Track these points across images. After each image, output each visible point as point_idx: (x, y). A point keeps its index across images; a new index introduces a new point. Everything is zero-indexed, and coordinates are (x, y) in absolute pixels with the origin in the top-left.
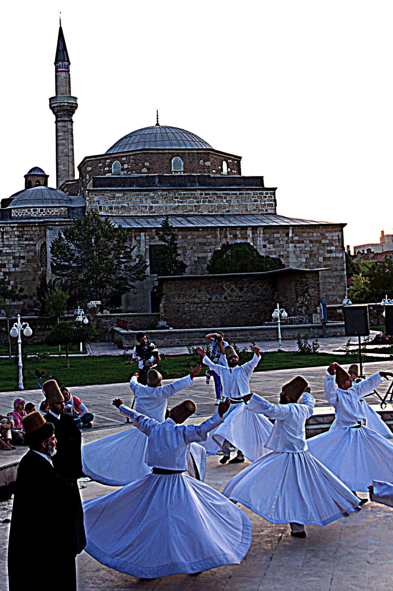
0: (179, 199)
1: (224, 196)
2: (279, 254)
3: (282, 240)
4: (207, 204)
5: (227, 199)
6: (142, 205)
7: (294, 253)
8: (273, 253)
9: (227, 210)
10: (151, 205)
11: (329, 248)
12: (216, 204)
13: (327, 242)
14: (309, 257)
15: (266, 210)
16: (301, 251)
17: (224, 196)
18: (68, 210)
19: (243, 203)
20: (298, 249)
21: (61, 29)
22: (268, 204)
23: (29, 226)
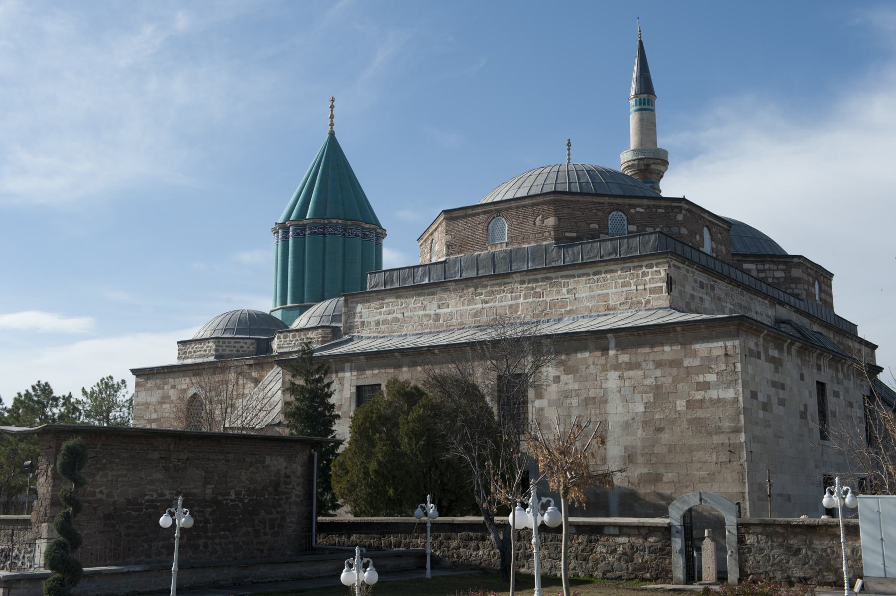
0: (483, 296)
1: (563, 281)
2: (585, 396)
3: (594, 364)
4: (530, 300)
5: (570, 287)
6: (422, 312)
7: (620, 392)
8: (574, 394)
9: (568, 309)
10: (438, 311)
11: (701, 379)
12: (548, 300)
13: (697, 362)
14: (652, 400)
15: (648, 302)
16: (635, 387)
17: (563, 281)
18: (333, 331)
19: (600, 292)
20: (627, 383)
21: (641, 42)
22: (650, 289)
23: (269, 363)
